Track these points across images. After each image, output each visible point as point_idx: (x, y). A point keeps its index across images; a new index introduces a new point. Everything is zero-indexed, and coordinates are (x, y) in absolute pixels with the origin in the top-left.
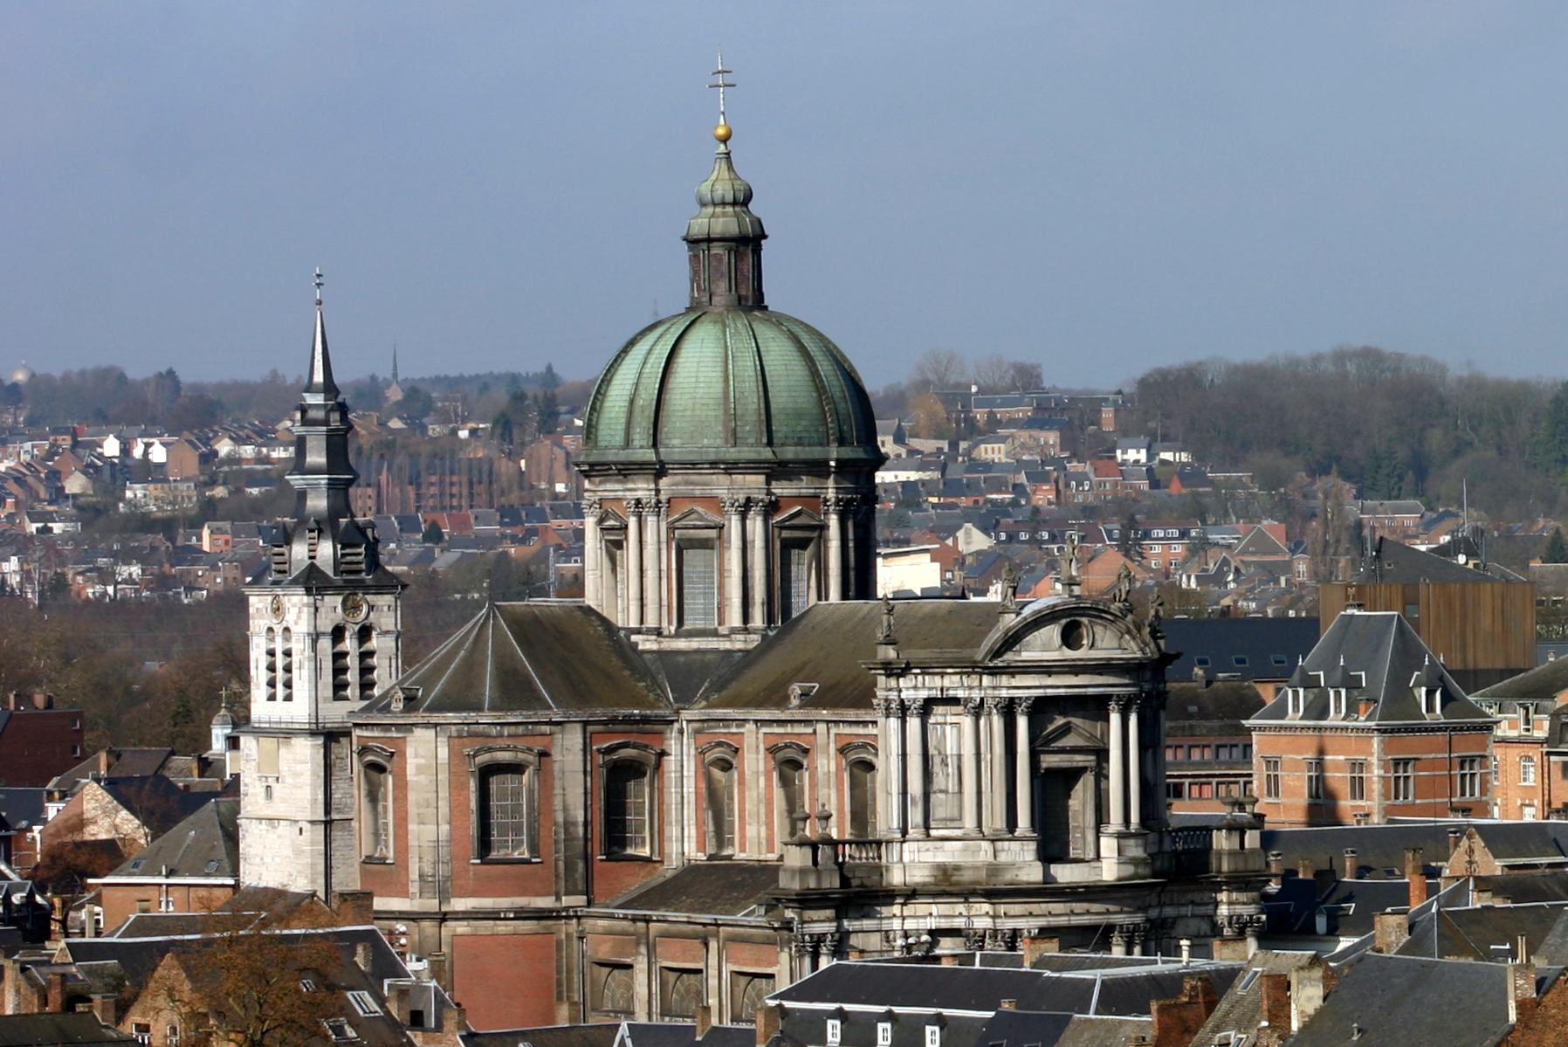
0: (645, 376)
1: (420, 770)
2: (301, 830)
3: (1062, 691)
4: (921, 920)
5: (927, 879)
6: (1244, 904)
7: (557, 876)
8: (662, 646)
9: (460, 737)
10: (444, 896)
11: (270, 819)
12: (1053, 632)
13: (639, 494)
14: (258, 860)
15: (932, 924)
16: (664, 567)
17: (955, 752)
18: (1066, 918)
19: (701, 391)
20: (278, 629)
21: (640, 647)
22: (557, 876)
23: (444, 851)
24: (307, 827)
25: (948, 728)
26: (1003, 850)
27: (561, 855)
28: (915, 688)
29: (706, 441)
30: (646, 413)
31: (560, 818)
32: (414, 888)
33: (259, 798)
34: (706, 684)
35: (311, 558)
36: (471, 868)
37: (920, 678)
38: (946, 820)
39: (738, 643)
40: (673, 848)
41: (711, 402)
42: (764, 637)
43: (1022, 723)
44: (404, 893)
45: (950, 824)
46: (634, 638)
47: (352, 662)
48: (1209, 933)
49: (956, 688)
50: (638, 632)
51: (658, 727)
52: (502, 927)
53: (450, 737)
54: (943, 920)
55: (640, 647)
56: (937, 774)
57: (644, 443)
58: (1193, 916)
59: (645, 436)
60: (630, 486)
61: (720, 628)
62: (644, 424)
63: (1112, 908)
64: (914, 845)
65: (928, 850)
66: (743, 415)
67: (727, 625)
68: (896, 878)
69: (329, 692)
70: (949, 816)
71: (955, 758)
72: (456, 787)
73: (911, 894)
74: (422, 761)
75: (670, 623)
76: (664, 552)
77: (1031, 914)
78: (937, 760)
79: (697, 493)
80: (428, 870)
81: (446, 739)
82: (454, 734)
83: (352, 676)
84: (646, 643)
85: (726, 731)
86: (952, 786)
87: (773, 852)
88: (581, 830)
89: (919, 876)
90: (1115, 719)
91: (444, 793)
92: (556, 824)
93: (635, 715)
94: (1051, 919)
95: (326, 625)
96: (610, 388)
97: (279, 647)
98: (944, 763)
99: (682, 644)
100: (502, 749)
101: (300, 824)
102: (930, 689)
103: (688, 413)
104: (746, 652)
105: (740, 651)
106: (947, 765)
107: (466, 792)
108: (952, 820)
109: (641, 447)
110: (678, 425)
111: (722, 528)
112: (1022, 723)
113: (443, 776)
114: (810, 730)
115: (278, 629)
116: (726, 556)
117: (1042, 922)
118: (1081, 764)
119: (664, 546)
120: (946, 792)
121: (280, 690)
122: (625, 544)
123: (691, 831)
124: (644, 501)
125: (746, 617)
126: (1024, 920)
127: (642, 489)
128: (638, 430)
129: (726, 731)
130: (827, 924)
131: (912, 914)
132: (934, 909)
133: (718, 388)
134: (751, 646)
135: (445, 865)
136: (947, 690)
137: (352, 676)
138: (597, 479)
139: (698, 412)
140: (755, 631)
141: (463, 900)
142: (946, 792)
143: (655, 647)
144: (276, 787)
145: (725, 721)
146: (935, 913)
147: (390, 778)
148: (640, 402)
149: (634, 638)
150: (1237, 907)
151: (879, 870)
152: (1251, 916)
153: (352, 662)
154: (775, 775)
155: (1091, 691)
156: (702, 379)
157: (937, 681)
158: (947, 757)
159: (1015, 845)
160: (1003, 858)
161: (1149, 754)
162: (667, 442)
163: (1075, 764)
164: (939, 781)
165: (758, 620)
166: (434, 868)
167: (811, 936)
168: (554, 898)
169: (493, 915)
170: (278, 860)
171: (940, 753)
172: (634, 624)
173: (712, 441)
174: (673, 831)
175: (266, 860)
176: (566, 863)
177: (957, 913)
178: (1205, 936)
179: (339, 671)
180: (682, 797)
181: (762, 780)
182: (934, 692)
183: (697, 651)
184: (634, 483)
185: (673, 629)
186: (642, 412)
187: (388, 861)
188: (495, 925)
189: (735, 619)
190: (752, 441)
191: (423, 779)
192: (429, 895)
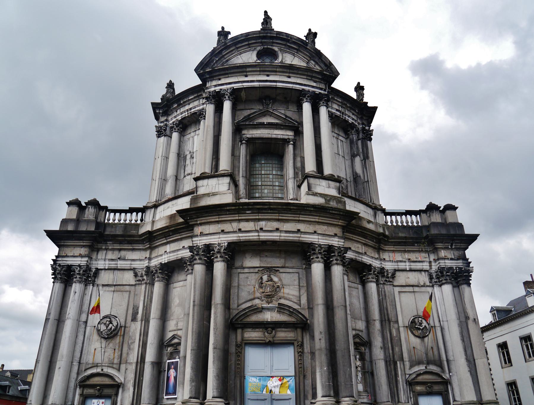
3: (256, 84)
4: (159, 258)
6: (452, 259)
15: (165, 259)
18: (257, 234)
26: (203, 186)
43: (227, 105)
48: (428, 283)
54: (172, 254)
56: (188, 165)
58: (411, 270)
63: (302, 227)
65: (168, 207)
78: (188, 157)
90: (307, 107)
94: (240, 235)
98: (192, 157)
106: (193, 158)
112: (227, 105)
117: (233, 237)
118: (282, 137)
126: (217, 236)
130: (79, 259)
131: (156, 255)
132: (168, 248)
150: (446, 261)
152: (460, 268)
155: (280, 85)
158: (193, 153)
159: (213, 182)
160: (201, 191)
161: (358, 160)
163: (274, 136)
171: (190, 153)
177: (181, 248)
178: (424, 286)
182: (184, 114)
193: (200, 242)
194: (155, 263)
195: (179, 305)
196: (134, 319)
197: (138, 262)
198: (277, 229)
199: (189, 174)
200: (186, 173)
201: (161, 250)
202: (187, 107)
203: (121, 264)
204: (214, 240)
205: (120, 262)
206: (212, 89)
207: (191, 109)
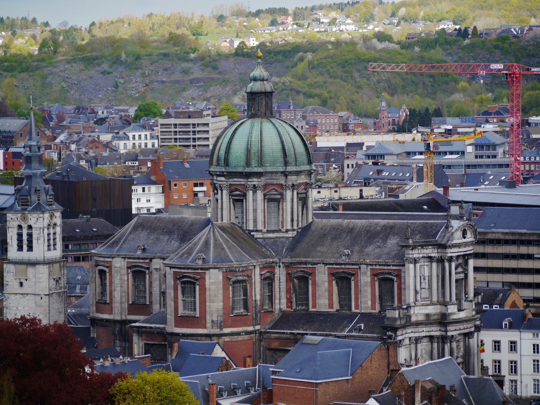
0: (253, 141)
1: (211, 284)
2: (41, 297)
4: (420, 333)
5: (423, 319)
7: (253, 319)
8: (264, 236)
9: (226, 272)
10: (221, 329)
11: (22, 294)
12: (459, 234)
13: (254, 183)
14: (14, 308)
15: (424, 334)
16: (263, 209)
17: (428, 275)
19: (274, 147)
20: (25, 226)
21: (255, 237)
22: (253, 319)
23: (221, 313)
24: (43, 297)
25: (425, 267)
27: (254, 312)
28: (419, 254)
29: (278, 165)
30: (257, 155)
31: (254, 299)
32: (209, 325)
33: (15, 287)
34: (284, 250)
35: (38, 200)
36: (230, 318)
37: (420, 250)
38: (425, 298)
39: (290, 234)
40: (277, 307)
41: (278, 150)
42: (298, 232)
44: (205, 327)
45: (426, 300)
46: (252, 233)
47: (52, 237)
49: (431, 253)
50: (253, 231)
51: (274, 264)
52: (240, 338)
53: (223, 272)
54: (427, 333)
55: (255, 237)
57: (256, 165)
59: (257, 163)
60: (250, 180)
61: (282, 229)
62: (256, 159)
64: (418, 308)
66: (290, 155)
67: (285, 228)
68: (413, 319)
69: (46, 248)
70: (426, 297)
71: (428, 277)
72: (225, 289)
73: (418, 324)
74: (213, 281)
75: (265, 228)
76: (263, 203)
77: (456, 330)
78: (422, 278)
79: (275, 182)
80: (215, 319)
81: (221, 273)
82: (225, 271)
83: (52, 242)
84: (257, 235)
85: (305, 266)
86: (427, 287)
87: (333, 308)
88: (259, 302)
89: (421, 318)
91: (221, 292)
92: (253, 300)
93: (270, 261)
95: (46, 224)
96: (231, 145)
97: (25, 232)
98: (424, 279)
99: (271, 235)
100: (240, 276)
101: (41, 296)
102: (423, 254)
103: (271, 155)
104: (293, 237)
105: (291, 237)
107: (228, 291)
108: (427, 298)
109: (256, 167)
110: (268, 159)
111: (282, 194)
112: (453, 265)
113: (221, 286)
114: (357, 267)
115: (25, 226)
116: (284, 203)
117: (458, 332)
119: (263, 201)
120: (425, 289)
121: (25, 247)
122: (244, 200)
123: (284, 301)
124: (257, 186)
125: (292, 225)
126: (454, 332)
127: (255, 181)
128: (253, 161)
129: (305, 266)
132: (424, 329)
133: (279, 146)
134: (294, 236)
135: (221, 317)
136: (429, 254)
137: (52, 242)
138: (228, 177)
139: (274, 154)
140: (294, 230)
141: (228, 329)
142: (425, 289)
143: (261, 236)
144: (25, 283)
145: (306, 263)
146: (425, 331)
147: (197, 287)
148: (253, 151)
149: (252, 233)
151: (410, 317)
153: (52, 237)
154: (334, 282)
156: (274, 143)
157: (425, 250)
162: (264, 165)
164: (423, 285)
165: (295, 227)
166: (218, 318)
167: (399, 340)
168: (252, 327)
169: (238, 334)
170: (26, 308)
172: (251, 228)
173: (280, 164)
174: (277, 301)
175: (19, 308)
176: (255, 314)
179: (49, 240)
180: (280, 289)
181: (326, 284)
183: (276, 237)
184: (251, 179)
185: (266, 230)
186: (255, 154)
187: (196, 316)
188: (238, 337)
189: (289, 227)
190: (293, 164)
191: (213, 287)
192: (216, 328)
193: (450, 334)
194: (417, 335)
195: (425, 353)
196: (411, 359)
197: (411, 334)
198: (467, 328)
199: (423, 288)
200: (422, 287)
201: (420, 329)
202: (425, 251)
203: (407, 335)
204: (454, 333)
205: (407, 335)
206: (449, 255)
207: (429, 254)
